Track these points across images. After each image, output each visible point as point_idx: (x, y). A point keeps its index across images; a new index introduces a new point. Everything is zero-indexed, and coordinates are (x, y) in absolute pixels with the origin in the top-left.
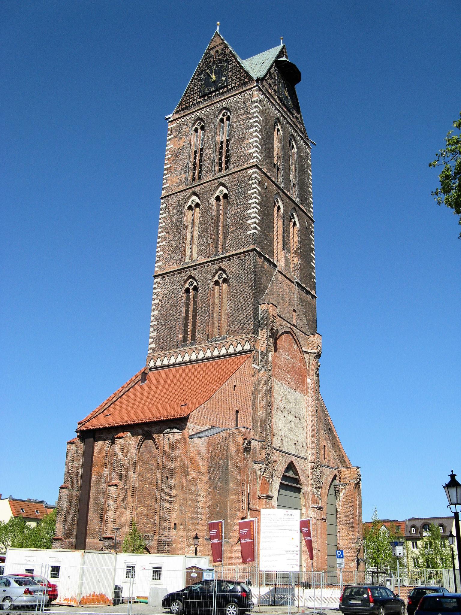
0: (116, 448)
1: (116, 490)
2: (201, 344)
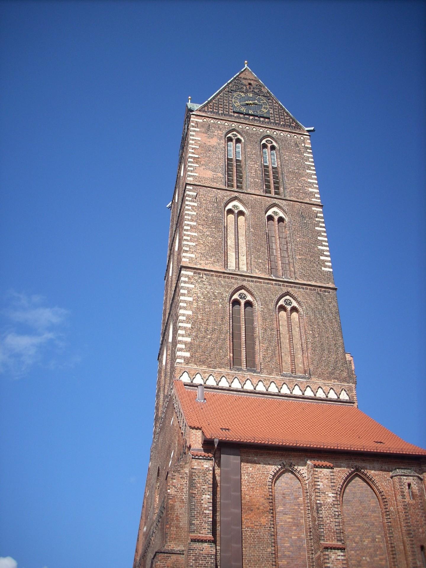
0: (318, 483)
1: (343, 558)
2: (270, 374)
